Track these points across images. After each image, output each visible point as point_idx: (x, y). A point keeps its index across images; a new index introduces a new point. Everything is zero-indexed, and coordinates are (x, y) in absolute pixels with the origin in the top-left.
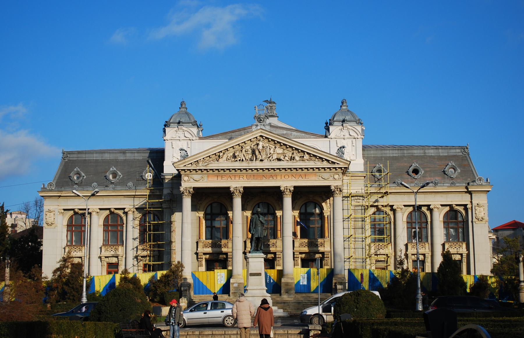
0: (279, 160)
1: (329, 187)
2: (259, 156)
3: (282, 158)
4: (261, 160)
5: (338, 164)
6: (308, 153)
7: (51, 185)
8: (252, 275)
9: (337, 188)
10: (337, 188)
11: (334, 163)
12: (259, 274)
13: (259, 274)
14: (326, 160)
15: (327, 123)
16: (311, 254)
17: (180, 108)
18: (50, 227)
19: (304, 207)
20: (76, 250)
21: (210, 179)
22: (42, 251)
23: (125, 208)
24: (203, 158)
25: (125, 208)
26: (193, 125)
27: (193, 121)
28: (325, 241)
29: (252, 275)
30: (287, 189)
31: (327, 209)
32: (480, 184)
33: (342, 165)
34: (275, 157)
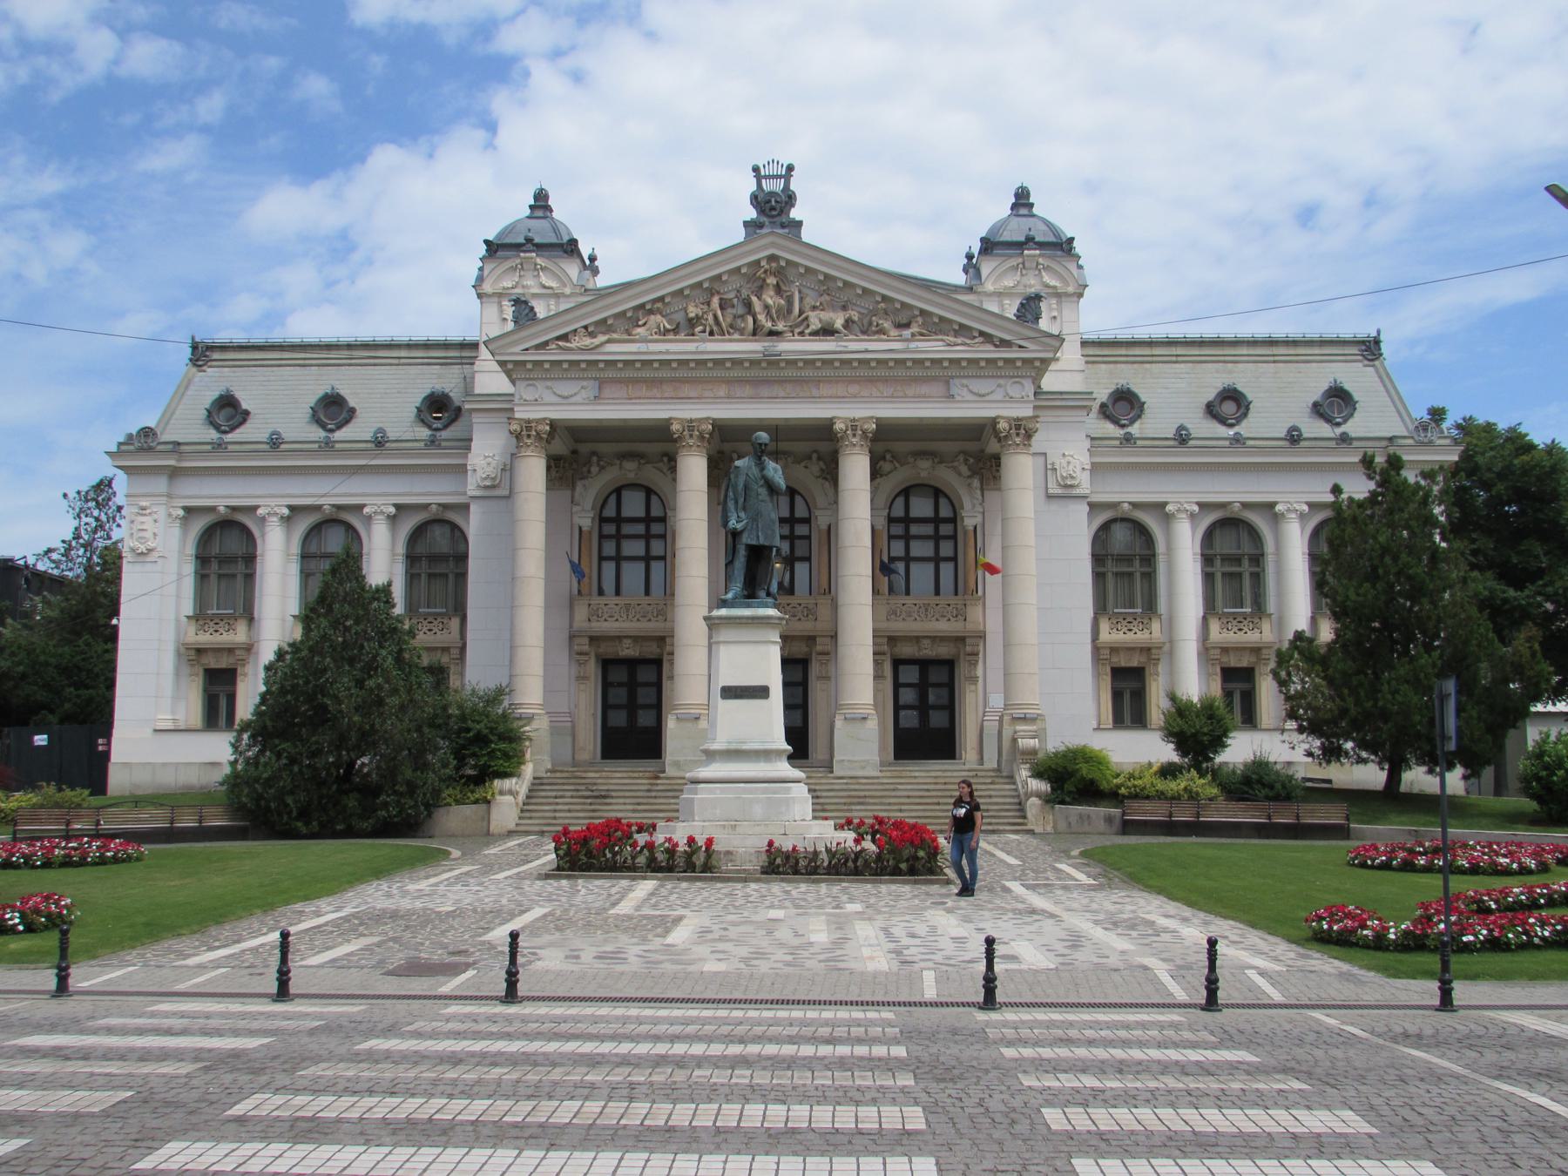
0: (827, 331)
1: (994, 422)
2: (761, 318)
3: (839, 323)
4: (772, 333)
5: (1020, 347)
6: (923, 312)
7: (146, 436)
8: (731, 693)
9: (1018, 427)
10: (1018, 427)
11: (1005, 343)
12: (761, 692)
13: (761, 692)
14: (982, 334)
15: (970, 257)
16: (926, 642)
17: (531, 207)
18: (141, 559)
19: (900, 501)
20: (216, 627)
21: (607, 392)
22: (116, 628)
23: (364, 506)
24: (586, 327)
25: (364, 506)
26: (566, 252)
27: (566, 239)
28: (968, 603)
29: (731, 693)
30: (854, 428)
31: (974, 506)
32: (1426, 440)
33: (1033, 351)
34: (815, 324)
